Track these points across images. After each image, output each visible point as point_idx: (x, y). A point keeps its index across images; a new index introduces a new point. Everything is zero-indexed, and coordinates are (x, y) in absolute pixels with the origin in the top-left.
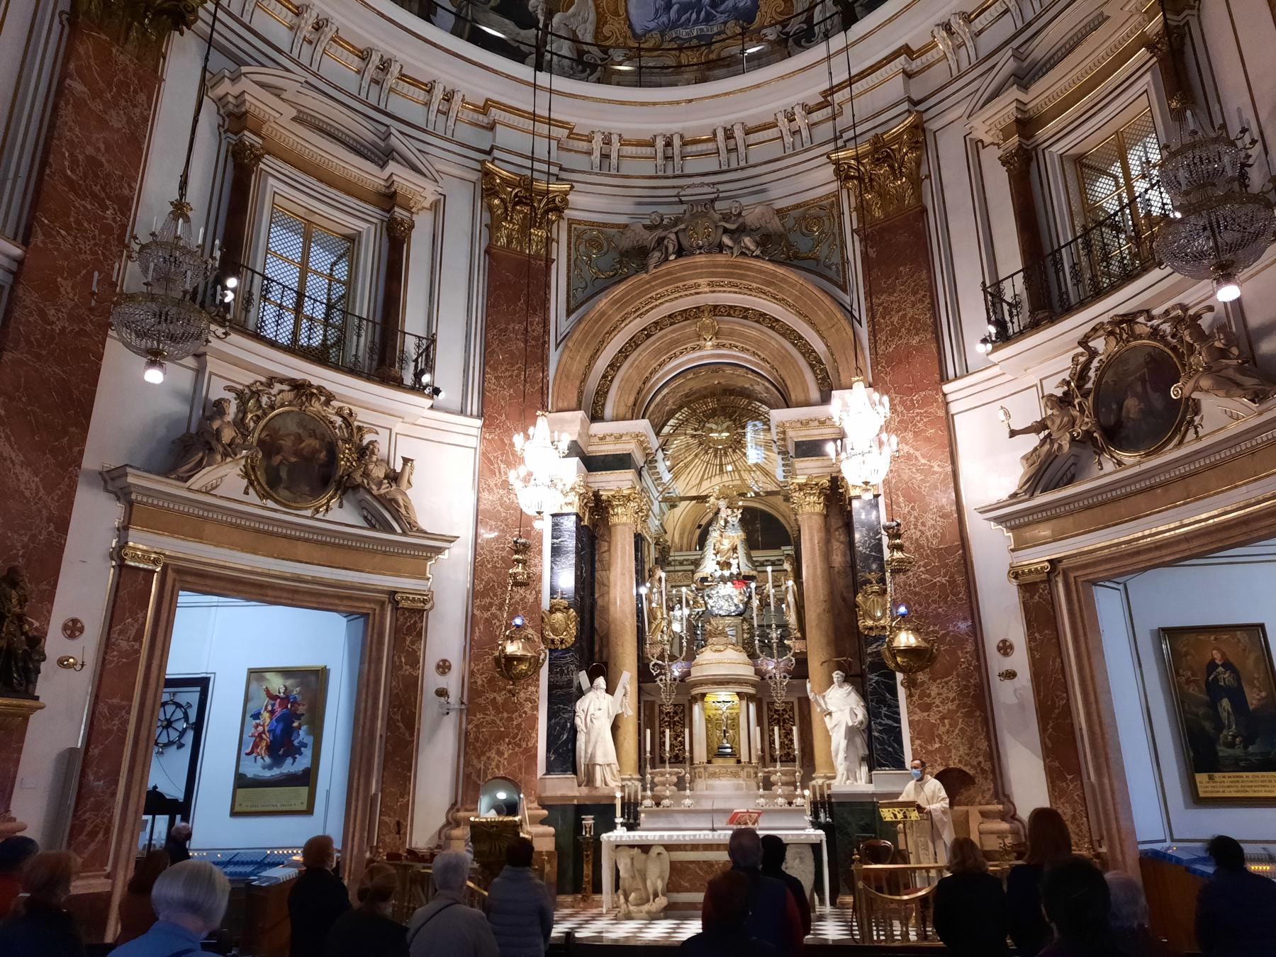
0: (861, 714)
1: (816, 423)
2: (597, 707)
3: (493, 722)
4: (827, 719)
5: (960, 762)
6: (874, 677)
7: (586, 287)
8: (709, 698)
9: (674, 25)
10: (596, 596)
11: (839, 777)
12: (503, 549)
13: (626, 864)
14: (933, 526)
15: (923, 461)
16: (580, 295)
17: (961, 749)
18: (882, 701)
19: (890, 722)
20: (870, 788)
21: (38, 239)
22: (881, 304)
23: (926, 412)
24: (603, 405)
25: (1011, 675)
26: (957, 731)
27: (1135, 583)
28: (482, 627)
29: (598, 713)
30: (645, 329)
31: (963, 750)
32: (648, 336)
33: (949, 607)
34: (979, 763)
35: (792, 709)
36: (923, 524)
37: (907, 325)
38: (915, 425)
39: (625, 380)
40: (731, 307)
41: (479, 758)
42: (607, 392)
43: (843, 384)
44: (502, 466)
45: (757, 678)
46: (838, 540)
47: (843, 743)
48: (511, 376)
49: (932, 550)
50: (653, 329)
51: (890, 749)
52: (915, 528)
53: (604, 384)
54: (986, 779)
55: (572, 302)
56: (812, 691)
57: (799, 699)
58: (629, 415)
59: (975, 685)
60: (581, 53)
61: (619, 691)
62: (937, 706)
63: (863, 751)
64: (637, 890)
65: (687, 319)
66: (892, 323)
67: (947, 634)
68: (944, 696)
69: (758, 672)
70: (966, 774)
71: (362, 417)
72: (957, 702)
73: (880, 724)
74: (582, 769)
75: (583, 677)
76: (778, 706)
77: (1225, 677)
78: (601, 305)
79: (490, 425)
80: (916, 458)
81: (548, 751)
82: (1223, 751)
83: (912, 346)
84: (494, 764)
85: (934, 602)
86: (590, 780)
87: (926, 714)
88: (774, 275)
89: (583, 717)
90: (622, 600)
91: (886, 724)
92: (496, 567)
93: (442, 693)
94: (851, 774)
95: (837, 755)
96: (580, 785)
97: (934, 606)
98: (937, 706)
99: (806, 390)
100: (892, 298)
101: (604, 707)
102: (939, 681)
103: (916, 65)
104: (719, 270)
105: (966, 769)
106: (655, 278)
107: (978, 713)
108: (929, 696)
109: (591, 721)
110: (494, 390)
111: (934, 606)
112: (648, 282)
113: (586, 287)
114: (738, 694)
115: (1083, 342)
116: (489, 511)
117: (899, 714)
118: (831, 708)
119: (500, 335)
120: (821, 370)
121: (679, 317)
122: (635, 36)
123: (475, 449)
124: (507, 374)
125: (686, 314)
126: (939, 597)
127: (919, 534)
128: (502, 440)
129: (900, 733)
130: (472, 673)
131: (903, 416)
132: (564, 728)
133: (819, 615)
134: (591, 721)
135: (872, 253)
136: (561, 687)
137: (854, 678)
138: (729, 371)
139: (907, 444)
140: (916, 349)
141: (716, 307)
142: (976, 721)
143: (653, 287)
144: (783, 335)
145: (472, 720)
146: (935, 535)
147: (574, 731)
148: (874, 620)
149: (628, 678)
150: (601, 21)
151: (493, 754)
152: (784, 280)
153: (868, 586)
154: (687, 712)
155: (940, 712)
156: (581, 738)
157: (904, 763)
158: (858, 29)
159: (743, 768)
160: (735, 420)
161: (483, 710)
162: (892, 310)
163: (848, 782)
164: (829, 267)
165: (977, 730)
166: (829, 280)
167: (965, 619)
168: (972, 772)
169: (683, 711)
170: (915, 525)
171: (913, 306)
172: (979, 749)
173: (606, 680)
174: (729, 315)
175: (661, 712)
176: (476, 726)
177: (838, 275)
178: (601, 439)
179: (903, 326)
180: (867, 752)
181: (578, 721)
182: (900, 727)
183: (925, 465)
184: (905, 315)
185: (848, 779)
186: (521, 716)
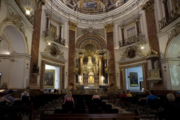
0: (104, 79)
9: (88, 7)
25: (118, 76)
27: (128, 69)
60: (78, 9)
71: (59, 47)
75: (78, 74)
77: (134, 77)
82: (133, 83)
86: (79, 83)
93: (66, 75)
94: (103, 84)
103: (113, 17)
115: (127, 48)
122: (84, 8)
125: (88, 39)
137: (104, 76)
147: (78, 79)
149: (82, 75)
150: (80, 6)
156: (79, 80)
158: (108, 13)
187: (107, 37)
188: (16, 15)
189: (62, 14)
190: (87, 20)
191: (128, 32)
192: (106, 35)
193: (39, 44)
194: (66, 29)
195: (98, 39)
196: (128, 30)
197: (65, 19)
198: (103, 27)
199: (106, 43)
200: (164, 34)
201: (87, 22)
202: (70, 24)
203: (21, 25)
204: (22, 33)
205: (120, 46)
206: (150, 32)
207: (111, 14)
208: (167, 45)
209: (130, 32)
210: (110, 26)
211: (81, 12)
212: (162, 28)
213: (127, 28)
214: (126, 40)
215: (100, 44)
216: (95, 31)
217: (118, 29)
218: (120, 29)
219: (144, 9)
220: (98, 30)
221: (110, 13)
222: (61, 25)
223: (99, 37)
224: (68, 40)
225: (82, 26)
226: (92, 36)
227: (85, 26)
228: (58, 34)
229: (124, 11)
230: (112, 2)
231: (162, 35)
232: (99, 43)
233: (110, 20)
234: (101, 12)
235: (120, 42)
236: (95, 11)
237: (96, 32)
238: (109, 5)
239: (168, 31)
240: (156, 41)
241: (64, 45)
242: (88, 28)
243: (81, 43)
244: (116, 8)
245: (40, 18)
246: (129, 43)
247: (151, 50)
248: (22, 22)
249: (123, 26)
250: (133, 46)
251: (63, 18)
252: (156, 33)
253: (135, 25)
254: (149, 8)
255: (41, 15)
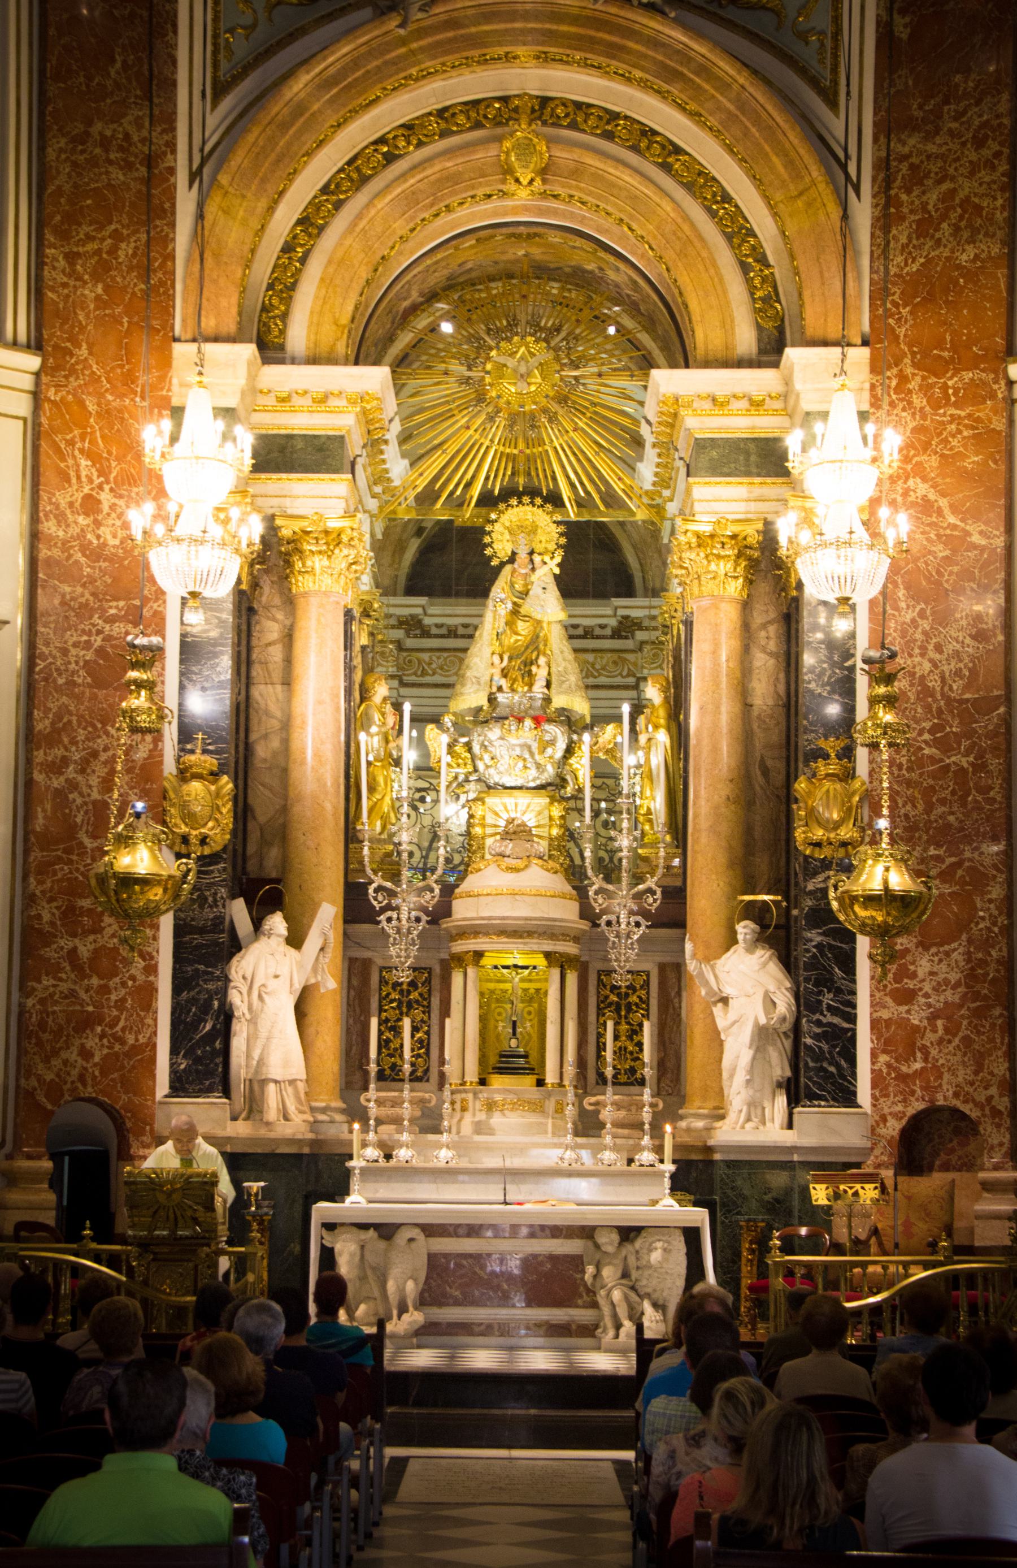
0: (784, 1004)
1: (744, 404)
2: (272, 971)
3: (72, 994)
4: (718, 1010)
5: (956, 1095)
6: (815, 936)
7: (254, 26)
8: (487, 961)
10: (253, 736)
11: (732, 1116)
12: (88, 645)
13: (352, 1255)
14: (957, 654)
15: (952, 519)
16: (241, 46)
17: (961, 1073)
18: (825, 981)
19: (836, 1020)
20: (789, 1138)
22: (905, 158)
23: (969, 416)
24: (285, 316)
26: (956, 1041)
28: (48, 807)
29: (272, 984)
30: (382, 140)
31: (963, 1074)
32: (390, 159)
33: (967, 815)
34: (989, 1099)
35: (646, 984)
36: (939, 648)
37: (954, 216)
38: (946, 441)
39: (339, 262)
40: (579, 105)
41: (47, 1060)
42: (293, 287)
43: (810, 332)
44: (84, 463)
45: (584, 925)
46: (764, 650)
47: (746, 1056)
48: (98, 252)
49: (949, 700)
50: (402, 143)
51: (832, 1069)
52: (923, 655)
53: (285, 268)
54: (998, 1126)
55: (224, 65)
56: (694, 956)
57: (662, 968)
58: (341, 348)
59: (998, 961)
61: (313, 942)
62: (927, 996)
63: (780, 1069)
64: (367, 1299)
65: (478, 125)
66: (924, 206)
67: (959, 864)
68: (940, 977)
69: (587, 913)
70: (964, 1116)
72: (962, 989)
73: (819, 1023)
74: (239, 1089)
75: (239, 911)
76: (621, 980)
78: (295, 89)
79: (57, 368)
80: (940, 512)
81: (174, 1051)
83: (959, 267)
84: (75, 1072)
85: (943, 802)
86: (253, 1107)
87: (903, 1008)
88: (684, 56)
89: (244, 990)
90: (316, 754)
91: (830, 1024)
92: (75, 684)
94: (755, 1110)
95: (732, 1076)
96: (234, 1118)
97: (941, 810)
98: (927, 996)
99: (727, 324)
100: (931, 148)
101: (284, 971)
102: (934, 950)
104: (564, 28)
105: (966, 1109)
106: (421, 33)
107: (997, 1011)
108: (914, 976)
109: (260, 997)
110: (65, 285)
111: (941, 810)
112: (403, 42)
113: (254, 26)
114: (548, 955)
116: (58, 563)
117: (854, 1006)
118: (728, 990)
119: (73, 150)
120: (764, 280)
121: (461, 119)
123: (25, 420)
124: (91, 247)
126: (953, 793)
127: (927, 666)
128: (82, 404)
129: (853, 1041)
130: (30, 899)
131: (924, 417)
132: (206, 1007)
133: (717, 807)
134: (260, 997)
136: (202, 931)
138: (555, 238)
139: (924, 479)
140: (971, 276)
141: (545, 101)
142: (993, 1026)
143: (413, 52)
144: (689, 187)
145: (34, 989)
146: (958, 673)
148: (825, 829)
151: (72, 1055)
152: (704, 70)
153: (821, 762)
154: (436, 982)
155: (929, 1006)
157: (855, 1094)
159: (549, 1095)
160: (556, 349)
161: (54, 971)
162: (927, 176)
163: (749, 1126)
164: (803, 36)
165: (992, 1040)
166: (803, 72)
167: (995, 839)
168: (974, 1114)
169: (428, 981)
170: (923, 649)
171: (972, 173)
172: (992, 1073)
173: (286, 918)
174: (573, 126)
175: (383, 981)
176: (42, 1001)
177: (821, 61)
178: (283, 400)
179: (944, 217)
180: (788, 1073)
181: (235, 998)
182: (854, 1032)
183: (955, 527)
184: (953, 192)
185: (748, 1119)
186: (124, 984)
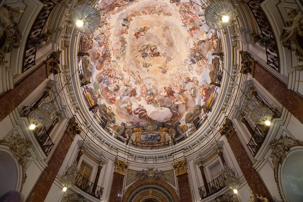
9: (148, 140)
21: (50, 164)
115: (216, 199)
125: (147, 188)
135: (180, 180)
150: (136, 138)
158: (176, 145)
187: (179, 182)
188: (24, 139)
189: (106, 149)
190: (146, 158)
191: (211, 172)
192: (176, 179)
193: (47, 193)
194: (108, 171)
195: (164, 187)
196: (211, 168)
197: (109, 155)
198: (171, 168)
199: (178, 194)
200: (263, 163)
201: (146, 160)
202: (117, 164)
203: (24, 155)
204: (19, 168)
205: (203, 198)
206: (243, 165)
207: (180, 148)
208: (277, 181)
209: (215, 172)
210: (183, 164)
211: (136, 146)
212: (255, 154)
213: (208, 164)
214: (210, 185)
215: (168, 197)
216: (157, 174)
217: (195, 168)
218: (197, 167)
219: (223, 134)
220: (162, 173)
221: (179, 145)
222: (101, 165)
223: (165, 183)
224: (110, 190)
225: (136, 166)
226: (152, 183)
227: (141, 167)
228: (92, 179)
229: (198, 141)
230: (181, 132)
231: (262, 165)
232: (166, 195)
233: (179, 156)
234: (167, 144)
235: (200, 189)
236: (157, 145)
237: (159, 175)
238: (176, 136)
239: (266, 158)
240: (257, 177)
241: (99, 198)
242: (146, 170)
243: (133, 197)
244: (187, 137)
245: (67, 150)
246: (216, 190)
247: (255, 196)
248: (30, 150)
249: (202, 162)
250: (224, 195)
251: (106, 154)
252: (252, 164)
253: (219, 158)
254: (228, 131)
255: (69, 147)
